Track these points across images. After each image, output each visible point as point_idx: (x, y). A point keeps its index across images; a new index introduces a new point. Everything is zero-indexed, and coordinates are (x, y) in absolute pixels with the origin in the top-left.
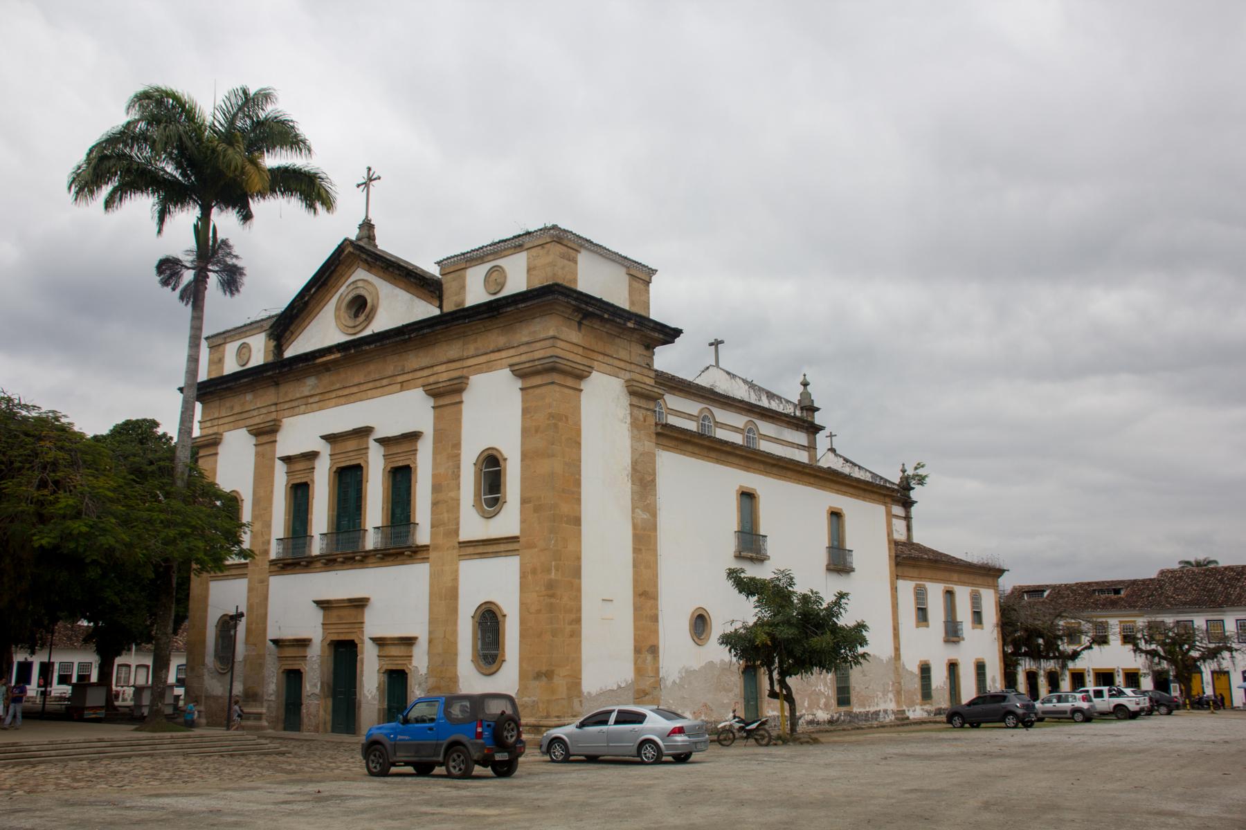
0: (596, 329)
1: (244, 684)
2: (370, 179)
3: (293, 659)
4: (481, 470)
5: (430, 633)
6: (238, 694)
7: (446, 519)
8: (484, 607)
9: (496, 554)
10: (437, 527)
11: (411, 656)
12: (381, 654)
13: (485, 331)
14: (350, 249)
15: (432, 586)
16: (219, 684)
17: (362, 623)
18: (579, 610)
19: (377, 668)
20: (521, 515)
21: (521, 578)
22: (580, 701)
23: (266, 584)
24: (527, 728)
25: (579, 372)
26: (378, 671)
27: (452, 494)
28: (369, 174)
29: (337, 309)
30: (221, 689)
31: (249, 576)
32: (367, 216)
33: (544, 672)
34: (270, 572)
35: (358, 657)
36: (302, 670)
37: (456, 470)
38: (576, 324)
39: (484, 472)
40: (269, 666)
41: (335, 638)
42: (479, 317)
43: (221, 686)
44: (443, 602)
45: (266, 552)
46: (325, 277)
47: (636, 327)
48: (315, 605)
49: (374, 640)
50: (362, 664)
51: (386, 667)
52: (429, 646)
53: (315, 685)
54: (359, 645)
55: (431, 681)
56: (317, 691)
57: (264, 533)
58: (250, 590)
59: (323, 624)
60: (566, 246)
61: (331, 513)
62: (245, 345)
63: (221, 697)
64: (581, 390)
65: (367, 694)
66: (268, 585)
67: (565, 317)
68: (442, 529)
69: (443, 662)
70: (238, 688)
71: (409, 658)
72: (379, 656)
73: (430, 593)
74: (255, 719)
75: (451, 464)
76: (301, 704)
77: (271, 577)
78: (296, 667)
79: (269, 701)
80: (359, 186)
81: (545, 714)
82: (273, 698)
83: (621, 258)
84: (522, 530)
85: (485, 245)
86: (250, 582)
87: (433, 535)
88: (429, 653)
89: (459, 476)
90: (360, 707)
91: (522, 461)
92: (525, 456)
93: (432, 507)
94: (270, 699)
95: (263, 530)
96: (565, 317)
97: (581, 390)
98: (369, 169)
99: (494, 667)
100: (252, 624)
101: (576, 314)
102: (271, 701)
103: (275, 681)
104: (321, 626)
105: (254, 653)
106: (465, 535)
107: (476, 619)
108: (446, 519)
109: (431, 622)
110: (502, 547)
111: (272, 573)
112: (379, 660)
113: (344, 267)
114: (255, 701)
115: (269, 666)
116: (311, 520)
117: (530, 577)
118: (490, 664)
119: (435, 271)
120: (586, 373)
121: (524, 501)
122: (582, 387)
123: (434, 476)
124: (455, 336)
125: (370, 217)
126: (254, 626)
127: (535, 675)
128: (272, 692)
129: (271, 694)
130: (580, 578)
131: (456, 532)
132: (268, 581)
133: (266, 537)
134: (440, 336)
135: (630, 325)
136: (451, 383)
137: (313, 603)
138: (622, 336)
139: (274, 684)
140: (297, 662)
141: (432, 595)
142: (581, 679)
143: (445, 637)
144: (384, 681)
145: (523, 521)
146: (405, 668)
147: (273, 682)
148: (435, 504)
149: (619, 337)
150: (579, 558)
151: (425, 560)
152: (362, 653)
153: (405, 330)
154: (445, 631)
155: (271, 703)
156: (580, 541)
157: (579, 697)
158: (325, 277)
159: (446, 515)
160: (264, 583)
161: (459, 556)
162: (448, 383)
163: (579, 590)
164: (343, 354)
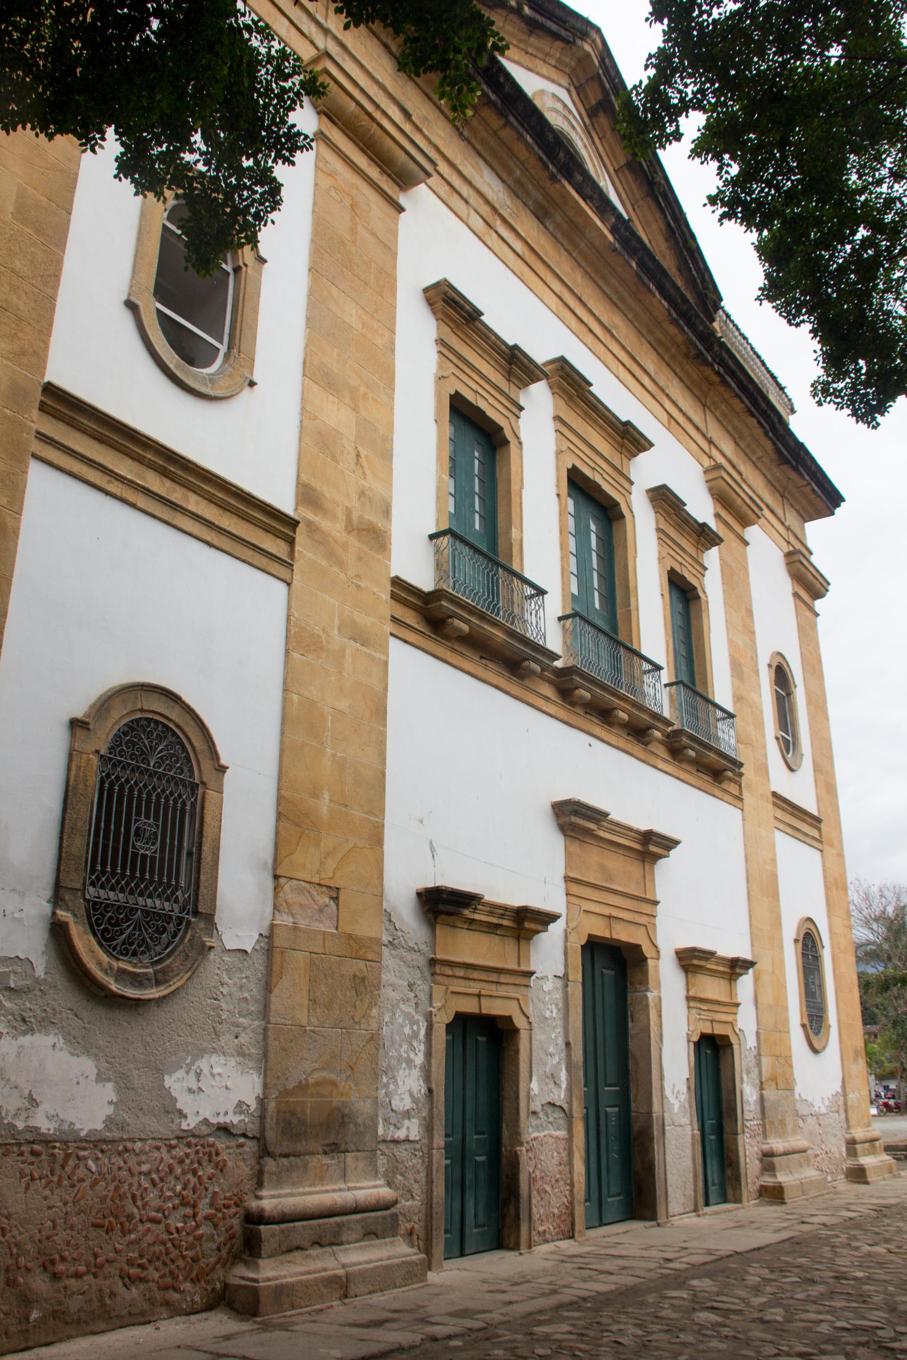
3: (494, 977)
6: (234, 1119)
12: (691, 994)
13: (754, 463)
16: (87, 1065)
17: (656, 903)
30: (108, 1091)
34: (395, 620)
36: (520, 1022)
40: (394, 995)
41: (600, 930)
42: (780, 446)
43: (101, 1078)
46: (549, 24)
53: (554, 1078)
56: (560, 1096)
59: (568, 879)
63: (96, 1142)
66: (386, 663)
71: (733, 1010)
72: (689, 999)
74: (371, 1233)
78: (495, 1008)
79: (396, 1142)
82: (412, 1129)
94: (401, 1134)
102: (407, 1140)
104: (562, 884)
105: (326, 927)
113: (558, 55)
114: (334, 1148)
115: (394, 995)
124: (730, 428)
128: (408, 1104)
129: (407, 1114)
132: (385, 650)
134: (723, 407)
136: (748, 501)
139: (416, 1073)
140: (502, 991)
143: (773, 972)
146: (729, 1032)
147: (409, 1061)
152: (658, 986)
153: (716, 348)
155: (402, 1153)
158: (549, 24)
161: (776, 818)
162: (748, 501)
164: (617, 245)
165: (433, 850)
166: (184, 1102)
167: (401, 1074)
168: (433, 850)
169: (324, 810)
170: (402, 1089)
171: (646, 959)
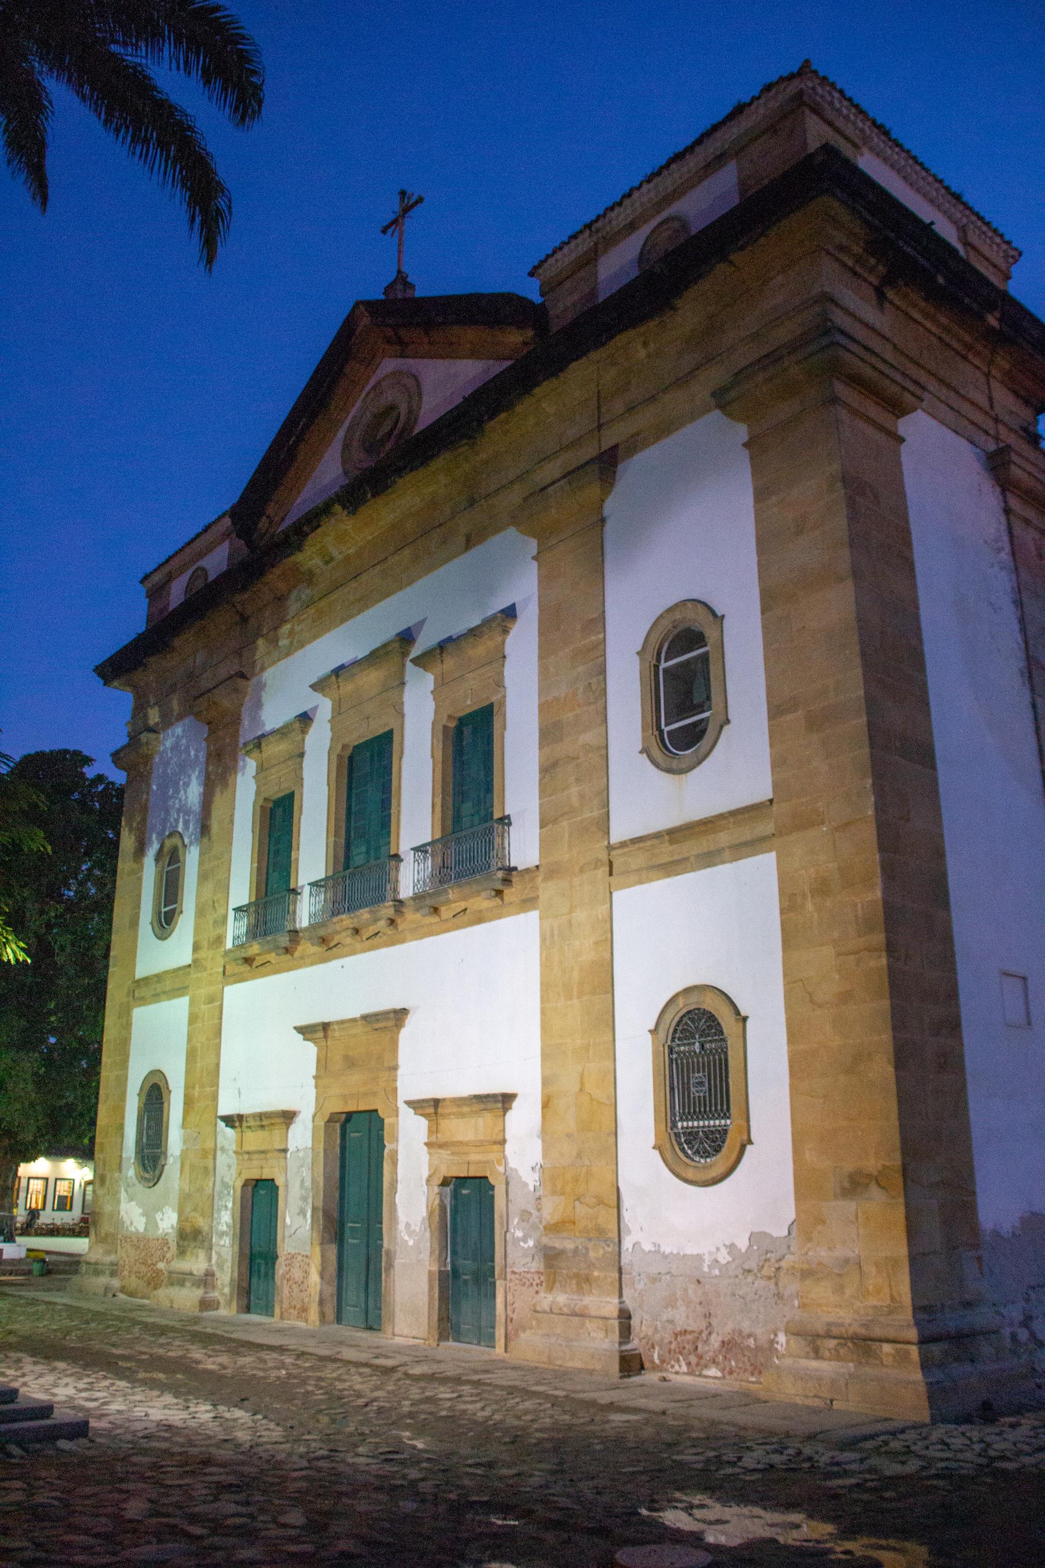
0: (916, 321)
1: (180, 1214)
2: (407, 210)
4: (657, 667)
5: (546, 1082)
7: (575, 800)
8: (681, 1002)
9: (709, 859)
10: (555, 821)
11: (503, 1142)
12: (433, 1139)
14: (362, 308)
15: (546, 965)
18: (952, 995)
19: (425, 1173)
20: (771, 746)
21: (783, 911)
22: (979, 1259)
23: (217, 1004)
24: (832, 1343)
25: (894, 389)
26: (428, 1181)
27: (589, 737)
28: (402, 199)
29: (346, 446)
30: (144, 1220)
31: (191, 993)
32: (399, 272)
33: (875, 1173)
35: (386, 1151)
36: (280, 1182)
37: (594, 680)
38: (871, 292)
39: (665, 671)
43: (143, 1215)
44: (575, 1001)
45: (220, 940)
47: (1005, 329)
48: (301, 1036)
49: (417, 1105)
50: (395, 1163)
51: (445, 1171)
52: (544, 1117)
54: (387, 1121)
55: (552, 1209)
57: (216, 904)
58: (193, 1019)
60: (830, 124)
61: (332, 839)
62: (199, 572)
64: (902, 440)
65: (406, 1238)
66: (221, 1006)
67: (844, 265)
68: (565, 823)
69: (579, 1155)
70: (168, 1221)
73: (542, 984)
75: (581, 669)
76: (277, 1257)
77: (228, 990)
80: (384, 231)
81: (888, 1302)
83: (949, 197)
84: (776, 786)
85: (636, 184)
86: (192, 1003)
87: (546, 844)
88: (545, 1133)
89: (604, 692)
90: (390, 1266)
91: (763, 613)
92: (769, 599)
93: (540, 780)
95: (215, 898)
96: (844, 265)
97: (902, 440)
98: (403, 193)
99: (718, 1163)
100: (194, 1088)
101: (873, 261)
103: (230, 1205)
106: (620, 830)
107: (662, 1034)
108: (575, 800)
109: (546, 1056)
110: (723, 838)
111: (229, 977)
112: (430, 1154)
116: (297, 860)
117: (810, 906)
118: (706, 1154)
119: (531, 291)
120: (908, 397)
121: (776, 711)
122: (901, 431)
123: (544, 708)
125: (405, 269)
126: (196, 1093)
127: (847, 1185)
128: (225, 1228)
130: (946, 905)
131: (604, 824)
133: (221, 911)
135: (992, 320)
137: (295, 1032)
138: (970, 356)
139: (229, 1212)
141: (546, 987)
142: (974, 1193)
143: (581, 1090)
144: (442, 1207)
145: (778, 763)
147: (226, 1207)
148: (548, 769)
149: (965, 358)
150: (939, 854)
151: (528, 903)
154: (582, 1075)
156: (937, 810)
157: (976, 1246)
159: (574, 790)
160: (216, 1000)
163: (948, 939)
165: (239, 1093)
166: (159, 1222)
167: (223, 1213)
168: (239, 1093)
169: (196, 1094)
170: (223, 1221)
171: (383, 1120)
